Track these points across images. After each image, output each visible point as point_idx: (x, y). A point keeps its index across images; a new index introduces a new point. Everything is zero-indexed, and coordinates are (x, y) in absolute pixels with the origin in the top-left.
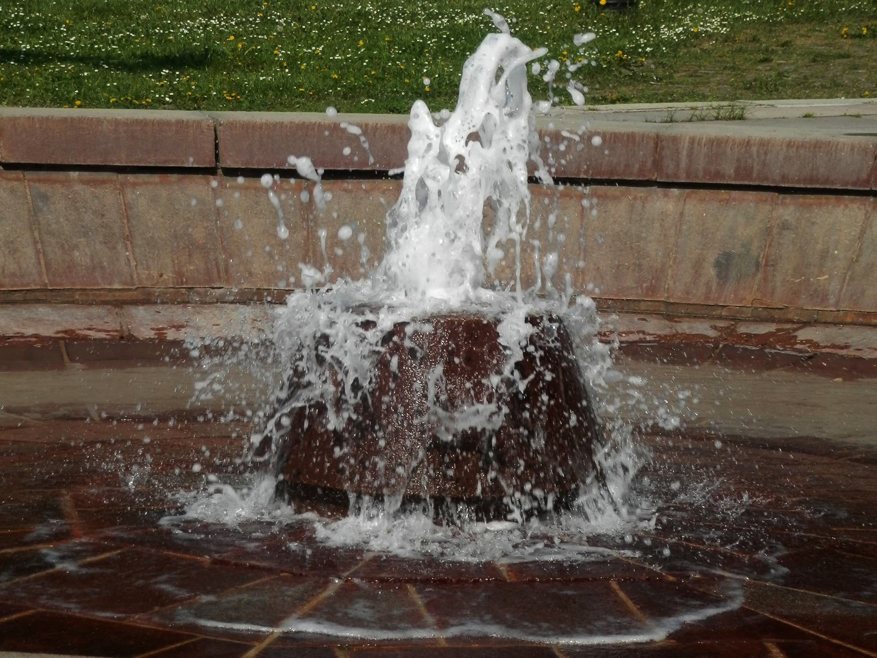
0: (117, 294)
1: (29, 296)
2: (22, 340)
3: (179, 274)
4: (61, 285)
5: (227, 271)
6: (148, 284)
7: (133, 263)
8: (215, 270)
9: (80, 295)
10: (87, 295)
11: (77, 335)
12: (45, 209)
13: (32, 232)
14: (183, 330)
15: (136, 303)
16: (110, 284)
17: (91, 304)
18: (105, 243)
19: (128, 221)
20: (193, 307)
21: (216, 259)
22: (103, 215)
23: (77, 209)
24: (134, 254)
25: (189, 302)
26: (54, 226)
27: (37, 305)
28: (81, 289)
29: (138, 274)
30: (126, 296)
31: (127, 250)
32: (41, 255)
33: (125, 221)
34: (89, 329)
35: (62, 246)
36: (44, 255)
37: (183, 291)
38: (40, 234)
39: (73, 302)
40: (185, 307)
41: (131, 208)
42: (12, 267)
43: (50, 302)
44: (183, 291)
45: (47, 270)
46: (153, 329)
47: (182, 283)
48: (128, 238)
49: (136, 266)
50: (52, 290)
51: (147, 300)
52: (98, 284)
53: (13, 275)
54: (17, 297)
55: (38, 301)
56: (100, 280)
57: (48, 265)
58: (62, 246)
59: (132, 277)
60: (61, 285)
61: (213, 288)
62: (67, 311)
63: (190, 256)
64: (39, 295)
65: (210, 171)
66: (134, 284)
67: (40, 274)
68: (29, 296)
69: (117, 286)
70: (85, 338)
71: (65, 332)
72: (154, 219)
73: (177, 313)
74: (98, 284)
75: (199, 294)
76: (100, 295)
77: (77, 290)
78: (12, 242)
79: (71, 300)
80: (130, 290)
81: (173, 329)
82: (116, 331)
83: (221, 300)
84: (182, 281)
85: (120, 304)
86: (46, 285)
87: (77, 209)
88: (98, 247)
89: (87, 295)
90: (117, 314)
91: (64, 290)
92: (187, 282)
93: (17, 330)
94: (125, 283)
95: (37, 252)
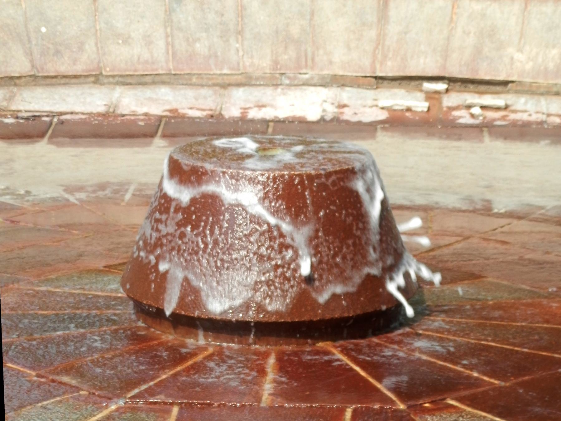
0: (225, 77)
1: (157, 79)
2: (133, 118)
3: (276, 62)
4: (182, 70)
5: (313, 60)
6: (249, 70)
7: (241, 53)
8: (304, 60)
9: (197, 78)
10: (202, 78)
11: (179, 114)
12: (178, 10)
13: (166, 27)
14: (264, 109)
15: (239, 85)
16: (221, 69)
17: (202, 86)
18: (221, 37)
19: (242, 20)
20: (283, 89)
21: (306, 51)
22: (223, 15)
23: (203, 10)
24: (242, 45)
25: (281, 85)
26: (183, 24)
27: (162, 86)
28: (197, 74)
29: (244, 62)
30: (233, 79)
31: (237, 42)
32: (170, 47)
33: (240, 20)
34: (191, 108)
35: (188, 40)
36: (172, 46)
37: (277, 76)
38: (172, 30)
39: (191, 85)
40: (276, 89)
41: (245, 9)
42: (146, 56)
43: (173, 84)
44: (277, 76)
45: (174, 57)
46: (241, 108)
47: (277, 69)
48: (240, 33)
49: (243, 55)
50: (175, 75)
51: (247, 81)
52: (211, 70)
53: (146, 62)
54: (148, 79)
55: (163, 83)
56: (213, 67)
57: (174, 54)
58: (188, 40)
59: (238, 64)
60: (182, 70)
61: (300, 74)
62: (182, 92)
63: (286, 48)
64: (165, 78)
66: (239, 70)
67: (167, 61)
68: (157, 79)
69: (225, 71)
70: (183, 117)
71: (170, 111)
72: (262, 18)
73: (265, 94)
74: (211, 70)
75: (289, 78)
76: (213, 79)
77: (194, 74)
78: (149, 36)
79: (189, 82)
80: (236, 74)
81: (256, 109)
82: (211, 110)
83: (306, 84)
84: (277, 67)
85: (225, 86)
86: (170, 70)
87: (203, 10)
88: (215, 40)
89: (202, 78)
90: (220, 95)
91: (184, 74)
92: (280, 69)
93: (133, 108)
94: (232, 69)
95: (167, 44)
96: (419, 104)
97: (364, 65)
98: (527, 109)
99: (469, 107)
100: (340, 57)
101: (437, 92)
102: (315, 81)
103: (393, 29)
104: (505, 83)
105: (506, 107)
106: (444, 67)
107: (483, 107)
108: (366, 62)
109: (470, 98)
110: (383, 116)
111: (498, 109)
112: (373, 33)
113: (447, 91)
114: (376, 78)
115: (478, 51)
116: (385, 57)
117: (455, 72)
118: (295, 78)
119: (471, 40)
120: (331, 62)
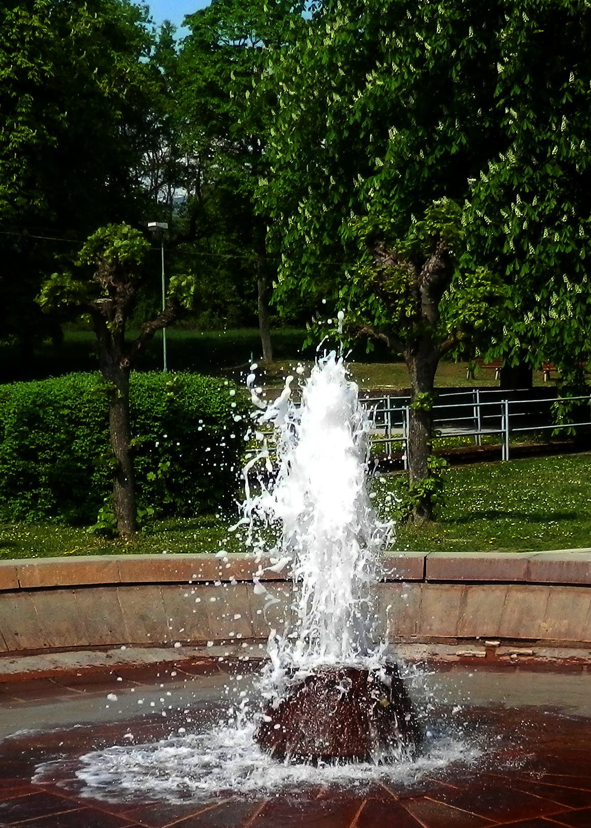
65: (422, 581)
96: (481, 653)
97: (450, 630)
98: (546, 654)
99: (511, 654)
100: (437, 625)
101: (494, 646)
102: (421, 641)
103: (469, 609)
104: (535, 641)
105: (534, 654)
106: (498, 632)
107: (519, 655)
108: (452, 629)
109: (512, 650)
110: (457, 659)
111: (529, 655)
112: (457, 612)
113: (499, 645)
114: (458, 638)
115: (520, 621)
116: (464, 626)
117: (506, 634)
118: (409, 639)
119: (516, 616)
120: (431, 629)
